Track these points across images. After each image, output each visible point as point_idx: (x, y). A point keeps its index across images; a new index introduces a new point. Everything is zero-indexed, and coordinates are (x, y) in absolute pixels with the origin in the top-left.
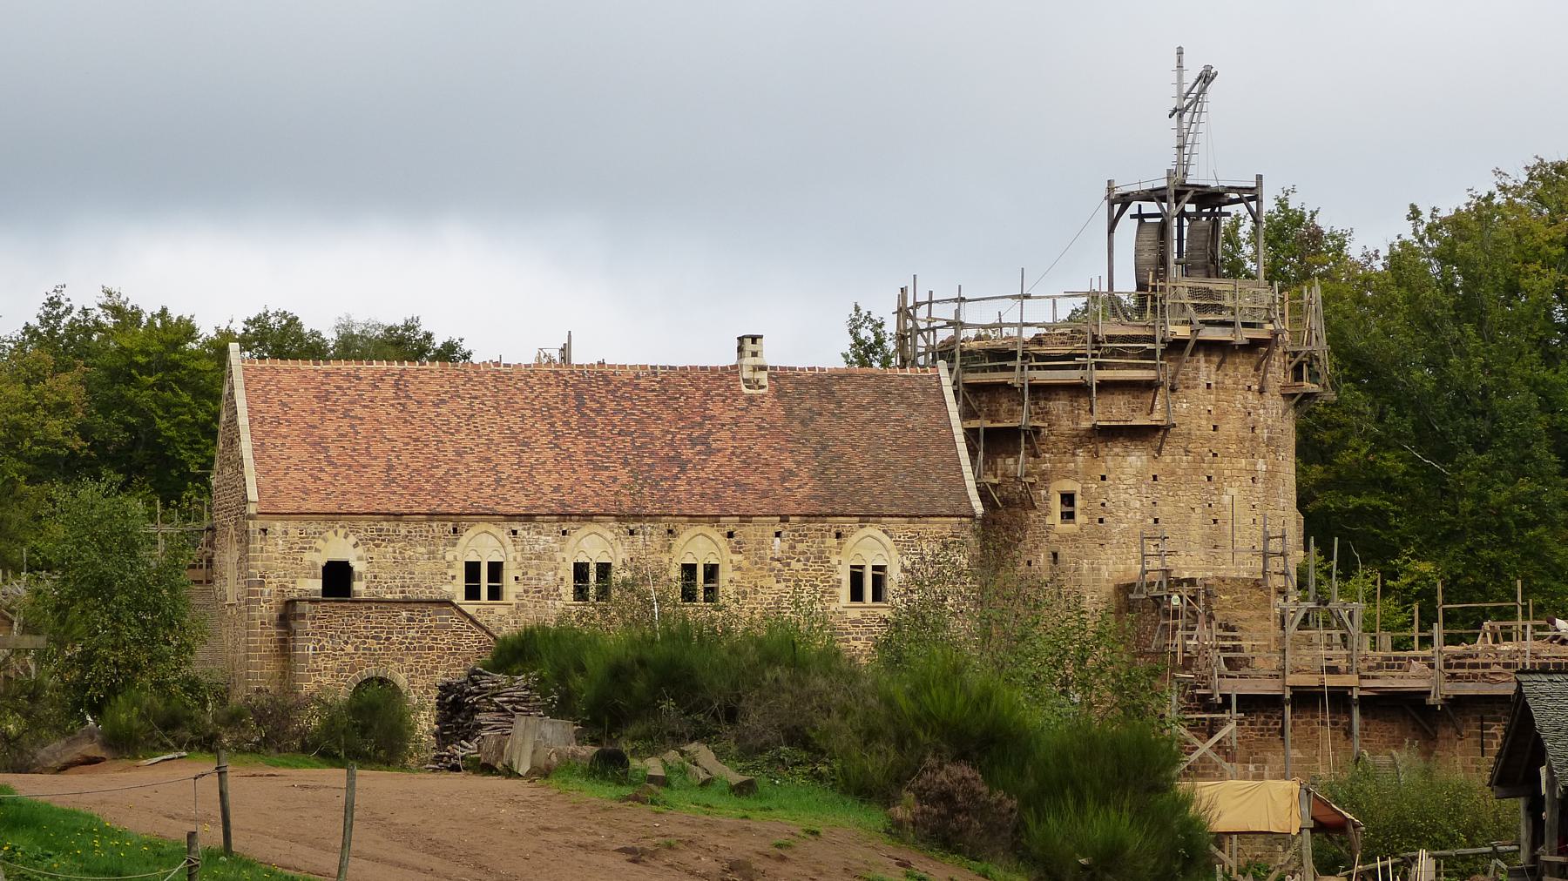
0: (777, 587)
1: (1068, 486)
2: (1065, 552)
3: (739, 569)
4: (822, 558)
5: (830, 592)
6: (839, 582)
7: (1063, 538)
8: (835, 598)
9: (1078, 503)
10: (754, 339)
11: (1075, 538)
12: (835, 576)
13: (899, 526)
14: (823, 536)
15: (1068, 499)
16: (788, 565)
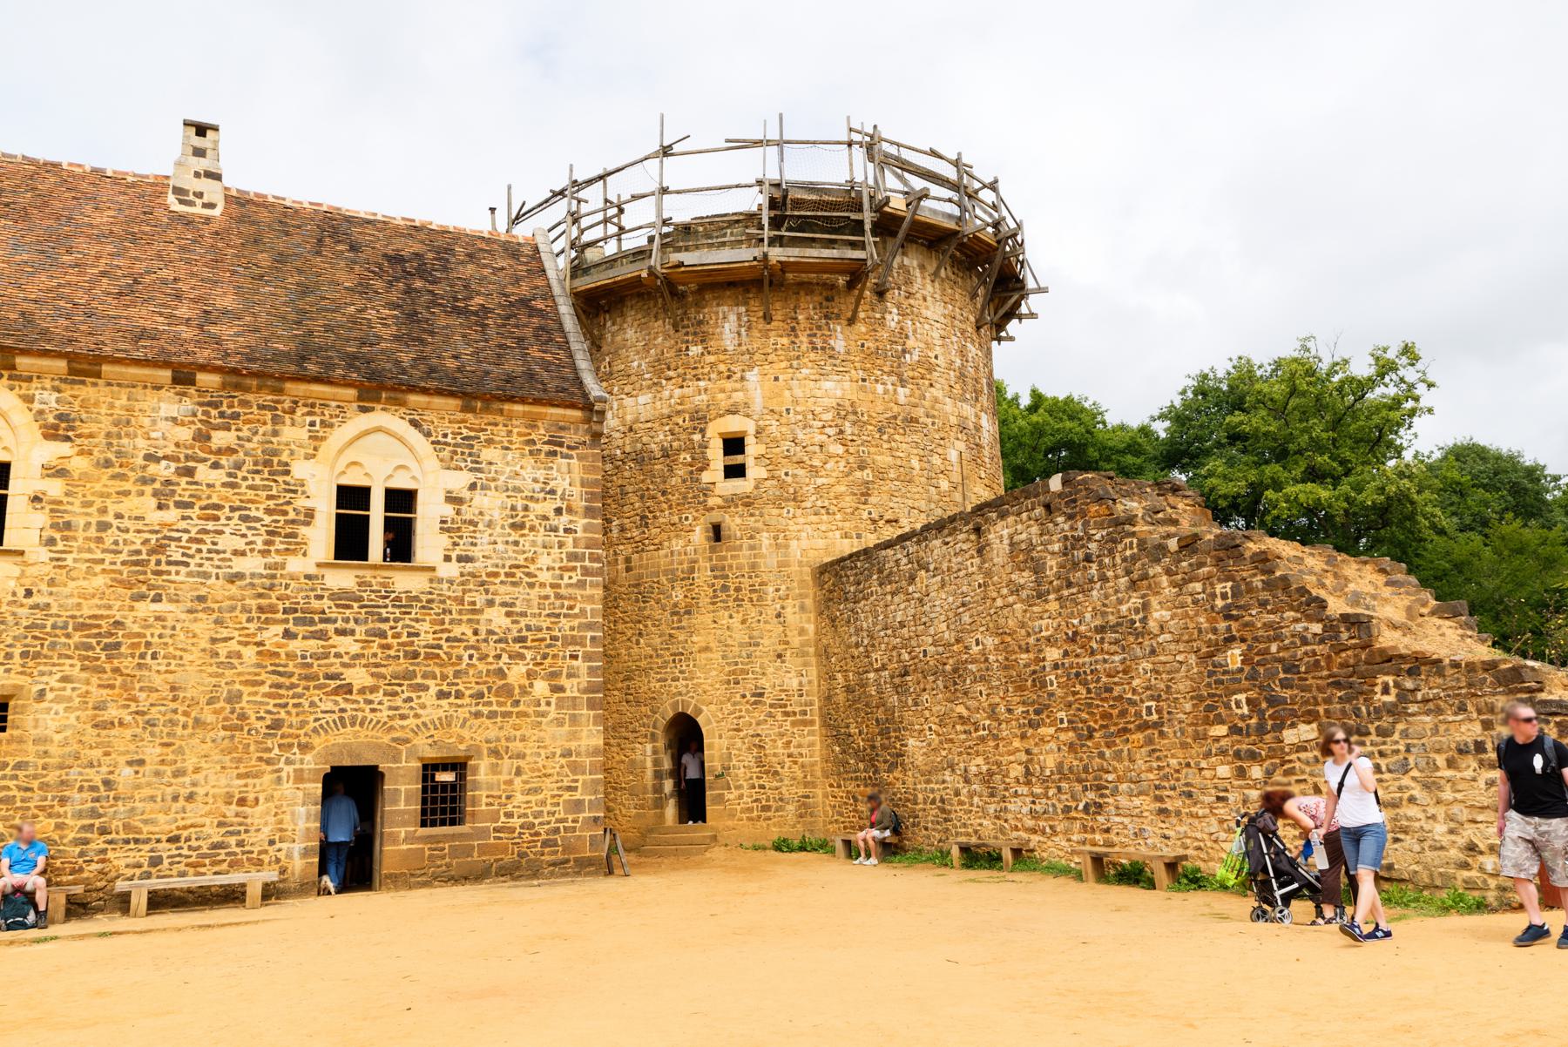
0: (155, 517)
1: (733, 425)
2: (733, 523)
3: (61, 473)
4: (273, 465)
5: (286, 535)
6: (310, 514)
7: (730, 502)
8: (295, 546)
9: (752, 448)
10: (201, 130)
11: (748, 502)
12: (301, 503)
13: (443, 412)
14: (276, 420)
15: (734, 445)
16: (190, 472)
